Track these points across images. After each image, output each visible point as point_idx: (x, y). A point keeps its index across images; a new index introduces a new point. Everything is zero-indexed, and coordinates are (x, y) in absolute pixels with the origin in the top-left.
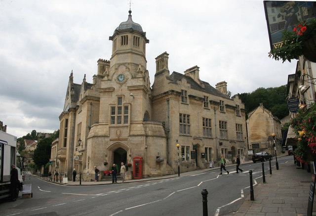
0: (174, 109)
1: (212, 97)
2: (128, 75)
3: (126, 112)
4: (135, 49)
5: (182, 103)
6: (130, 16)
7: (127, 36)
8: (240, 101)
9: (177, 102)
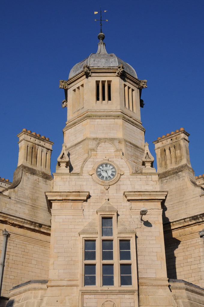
3: (125, 255)
7: (109, 82)
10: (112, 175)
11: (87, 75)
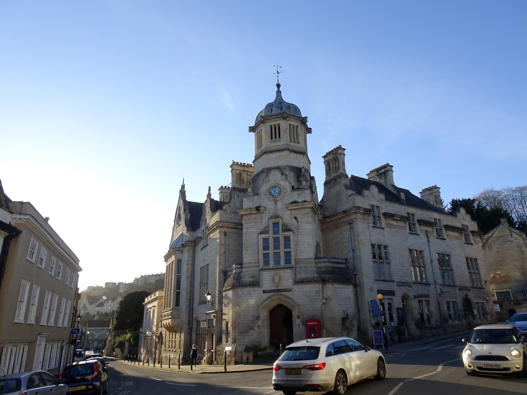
0: (361, 238)
1: (420, 214)
2: (286, 185)
4: (293, 144)
5: (373, 227)
6: (279, 92)
8: (468, 217)
9: (365, 225)
10: (279, 193)
11: (263, 122)
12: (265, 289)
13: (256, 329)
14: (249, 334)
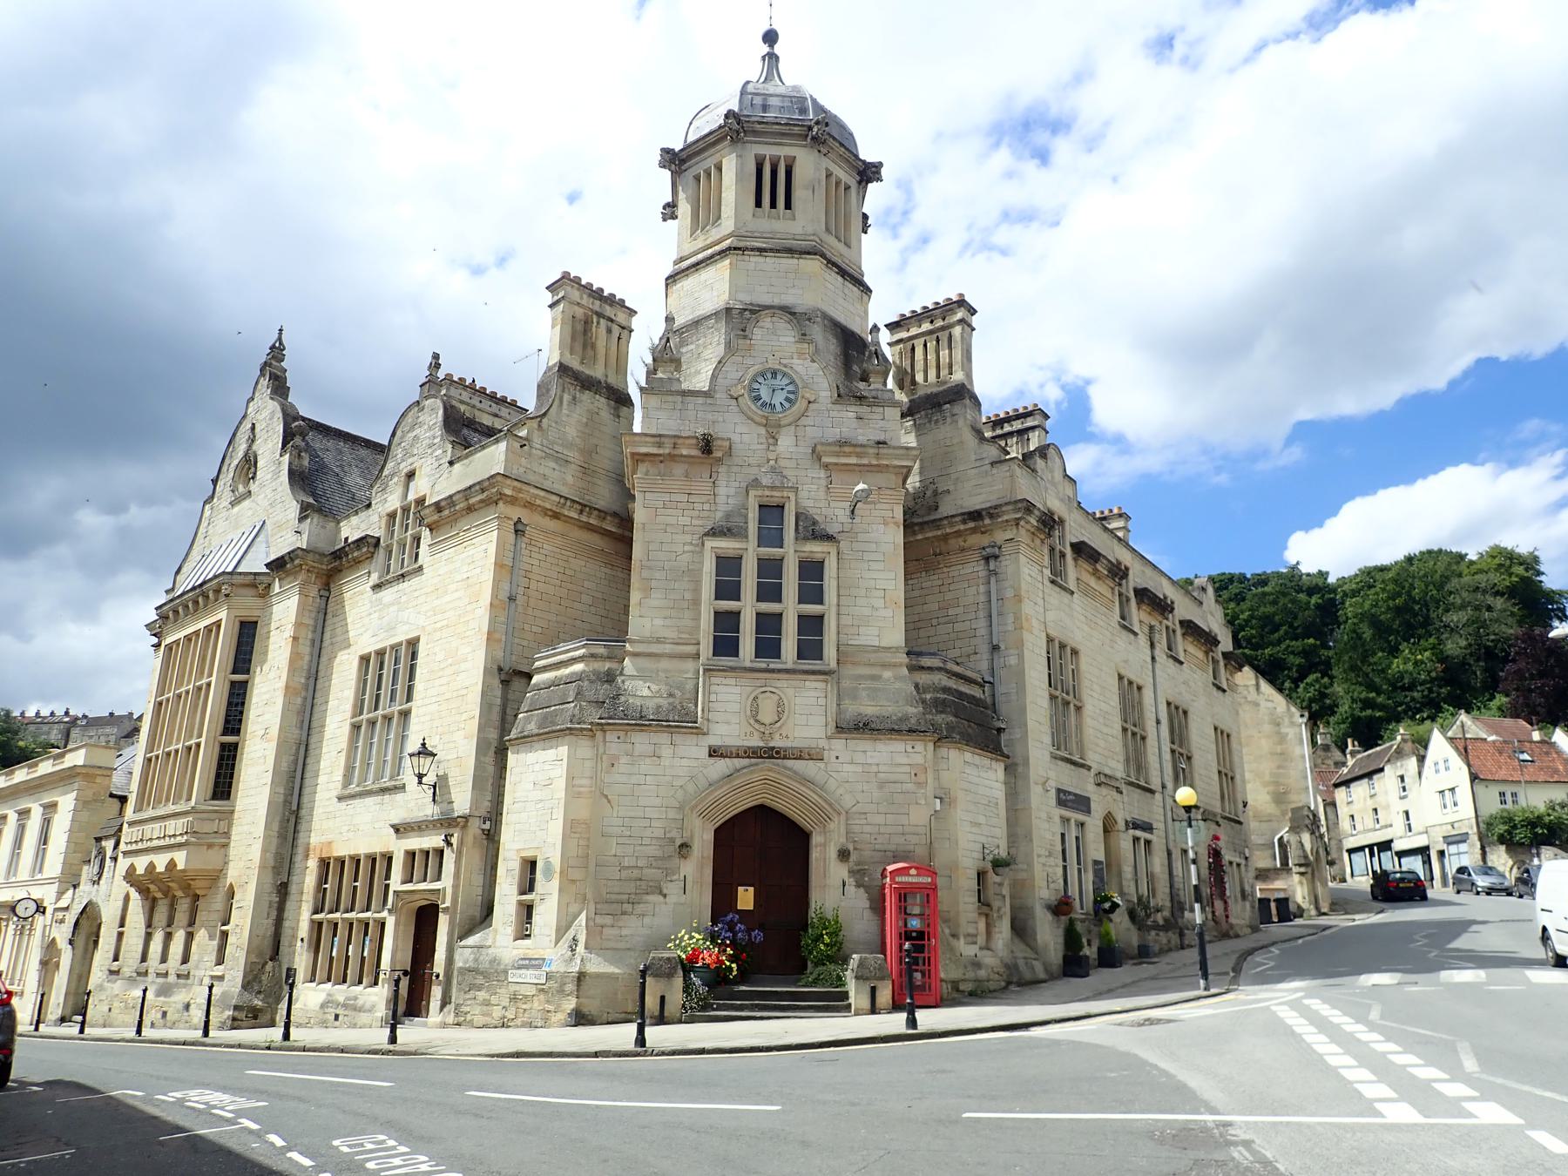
0: (1027, 608)
5: (1053, 582)
12: (714, 741)
13: (673, 889)
14: (639, 908)
